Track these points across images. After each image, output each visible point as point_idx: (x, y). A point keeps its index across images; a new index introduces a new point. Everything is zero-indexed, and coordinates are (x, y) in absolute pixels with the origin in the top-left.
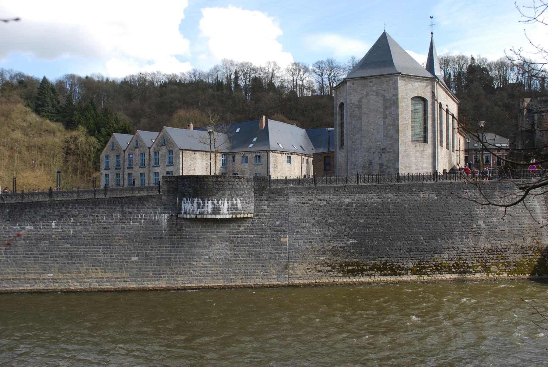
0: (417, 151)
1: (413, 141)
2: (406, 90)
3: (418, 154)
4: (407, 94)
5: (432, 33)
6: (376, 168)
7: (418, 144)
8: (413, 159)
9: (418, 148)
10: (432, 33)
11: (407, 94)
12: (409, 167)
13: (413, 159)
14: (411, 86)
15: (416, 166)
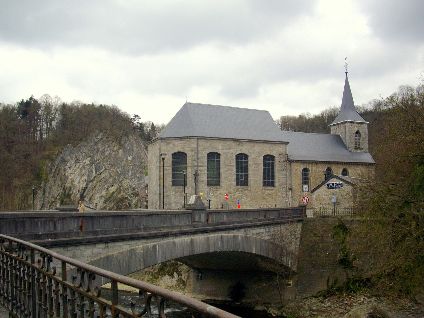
0: (176, 192)
1: (174, 185)
2: (167, 149)
3: (177, 194)
4: (168, 151)
5: (346, 73)
6: (154, 205)
7: (178, 187)
8: (173, 198)
9: (177, 190)
10: (346, 73)
11: (168, 151)
12: (170, 205)
13: (173, 198)
14: (172, 145)
15: (176, 203)
